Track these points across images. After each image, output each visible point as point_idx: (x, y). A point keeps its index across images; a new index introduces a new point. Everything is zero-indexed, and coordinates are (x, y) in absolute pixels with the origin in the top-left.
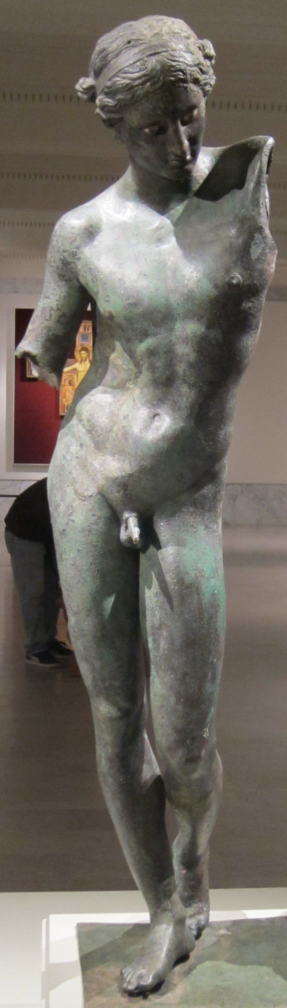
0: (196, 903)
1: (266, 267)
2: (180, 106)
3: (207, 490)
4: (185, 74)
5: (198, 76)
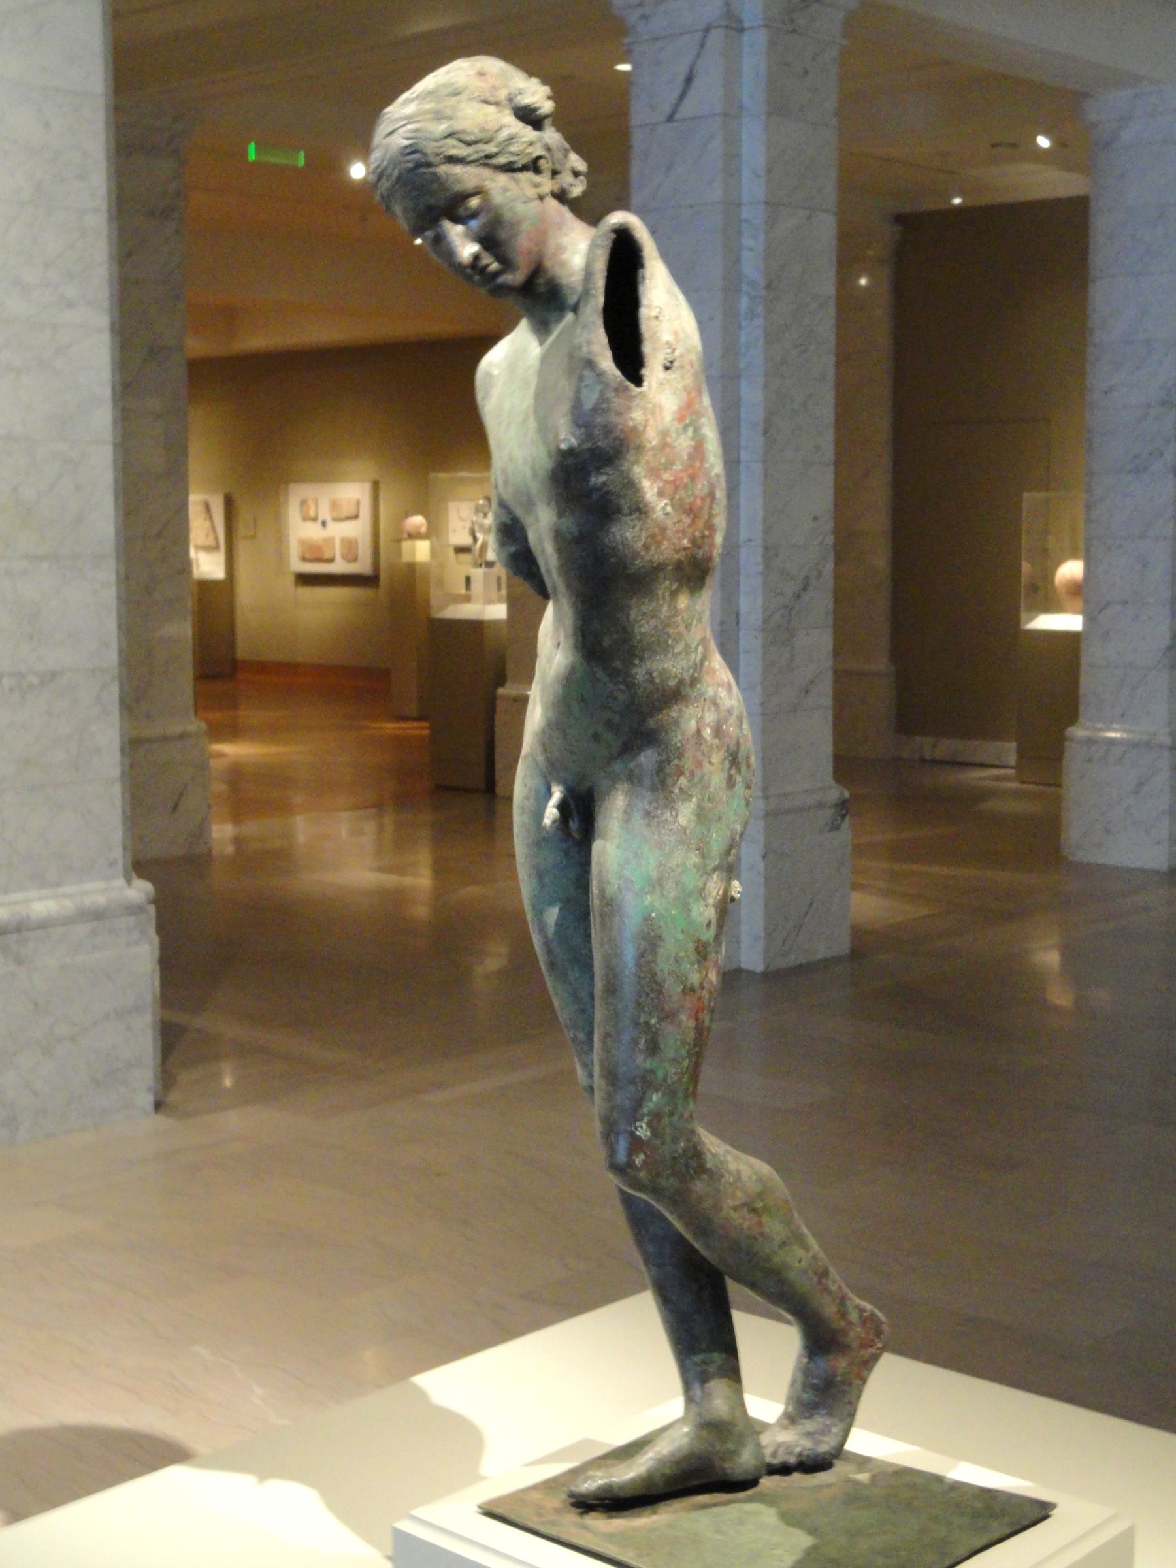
0: (822, 1416)
1: (613, 419)
2: (432, 201)
3: (647, 758)
4: (425, 155)
5: (453, 152)
